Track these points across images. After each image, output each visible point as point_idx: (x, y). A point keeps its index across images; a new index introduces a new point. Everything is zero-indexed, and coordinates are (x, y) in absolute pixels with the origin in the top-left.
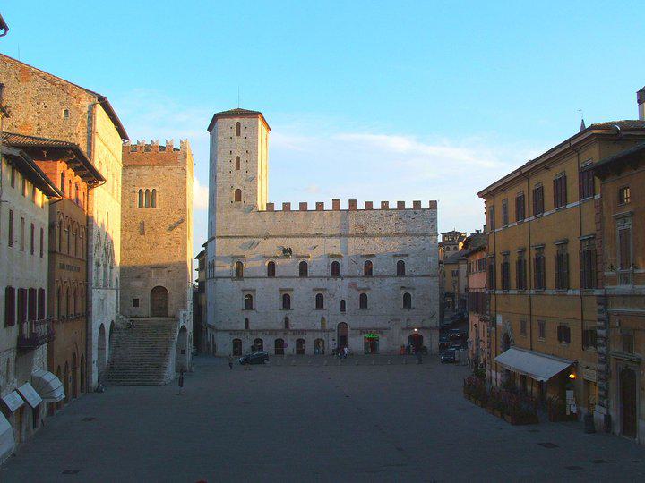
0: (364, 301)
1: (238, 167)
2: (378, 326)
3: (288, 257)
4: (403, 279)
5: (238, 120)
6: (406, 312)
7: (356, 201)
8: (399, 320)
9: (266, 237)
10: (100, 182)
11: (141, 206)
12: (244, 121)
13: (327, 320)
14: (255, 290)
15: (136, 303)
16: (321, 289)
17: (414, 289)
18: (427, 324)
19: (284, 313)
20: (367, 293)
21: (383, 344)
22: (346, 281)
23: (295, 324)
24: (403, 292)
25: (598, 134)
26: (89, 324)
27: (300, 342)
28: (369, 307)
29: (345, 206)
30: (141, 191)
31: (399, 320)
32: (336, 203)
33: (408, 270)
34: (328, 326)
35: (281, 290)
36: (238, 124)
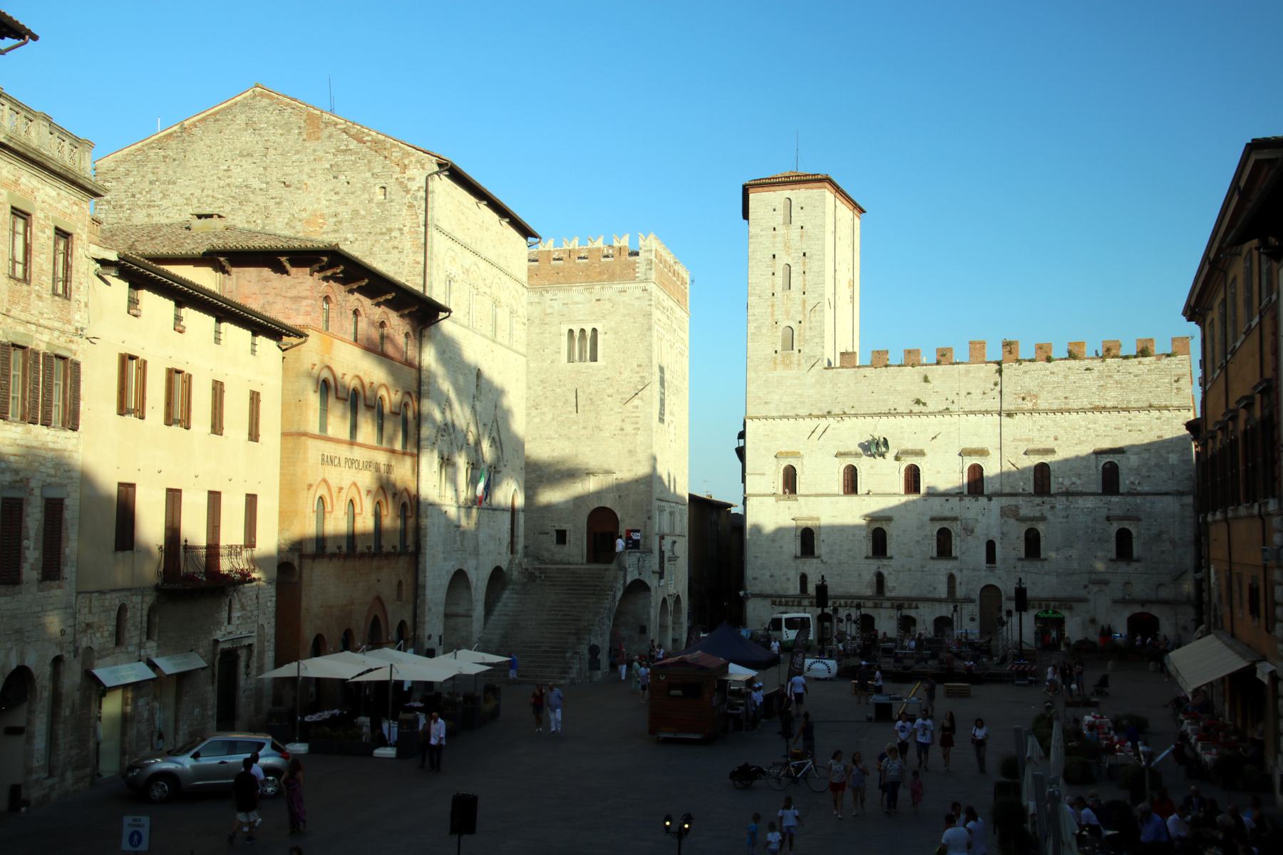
0: (1033, 544)
2: (1062, 594)
4: (1115, 499)
6: (1123, 567)
8: (1106, 583)
10: (442, 315)
11: (570, 360)
12: (800, 195)
13: (958, 580)
15: (561, 536)
16: (945, 519)
17: (1138, 519)
18: (1164, 593)
19: (874, 565)
20: (1041, 527)
21: (1074, 630)
22: (996, 504)
23: (897, 586)
24: (1115, 527)
25: (1269, 161)
26: (421, 567)
27: (907, 623)
28: (1042, 556)
30: (571, 331)
31: (1106, 583)
33: (1125, 482)
34: (960, 592)
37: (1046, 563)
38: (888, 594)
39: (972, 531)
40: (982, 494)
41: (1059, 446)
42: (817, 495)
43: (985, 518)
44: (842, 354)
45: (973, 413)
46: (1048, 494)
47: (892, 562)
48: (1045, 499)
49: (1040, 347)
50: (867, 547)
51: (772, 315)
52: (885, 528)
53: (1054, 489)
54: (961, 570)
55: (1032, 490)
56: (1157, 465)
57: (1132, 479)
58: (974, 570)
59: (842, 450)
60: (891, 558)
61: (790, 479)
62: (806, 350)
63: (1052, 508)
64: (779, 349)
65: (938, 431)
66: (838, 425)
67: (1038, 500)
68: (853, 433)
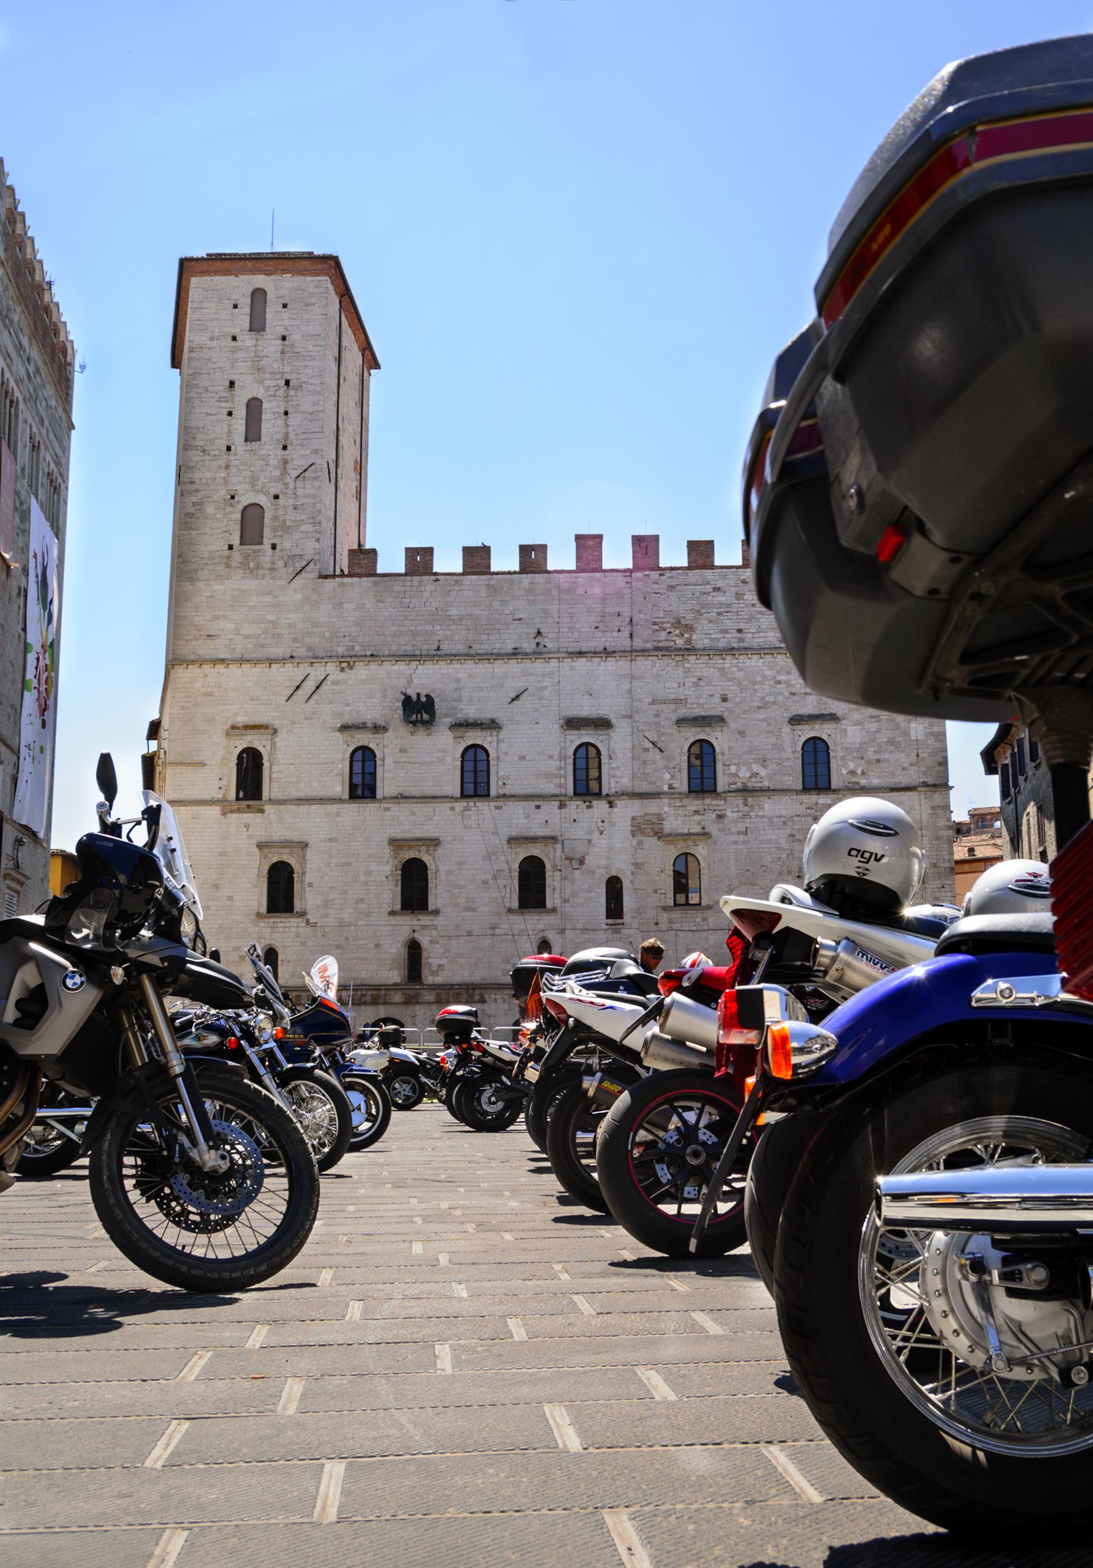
1: (253, 434)
3: (429, 723)
5: (260, 280)
7: (655, 539)
9: (347, 661)
14: (304, 845)
16: (533, 840)
19: (407, 925)
20: (701, 851)
22: (626, 811)
23: (443, 964)
29: (617, 556)
32: (588, 546)
35: (396, 844)
36: (258, 296)
37: (710, 913)
38: (428, 978)
39: (582, 862)
40: (599, 795)
41: (731, 711)
42: (300, 801)
43: (606, 840)
44: (351, 552)
45: (581, 654)
46: (713, 791)
47: (439, 921)
48: (708, 801)
49: (692, 545)
50: (390, 894)
51: (226, 483)
52: (426, 858)
53: (722, 784)
54: (562, 931)
55: (685, 788)
56: (891, 742)
57: (852, 766)
58: (585, 930)
59: (348, 719)
60: (436, 912)
61: (250, 774)
62: (286, 544)
63: (720, 817)
64: (236, 540)
65: (521, 686)
66: (342, 676)
67: (694, 804)
68: (370, 692)
